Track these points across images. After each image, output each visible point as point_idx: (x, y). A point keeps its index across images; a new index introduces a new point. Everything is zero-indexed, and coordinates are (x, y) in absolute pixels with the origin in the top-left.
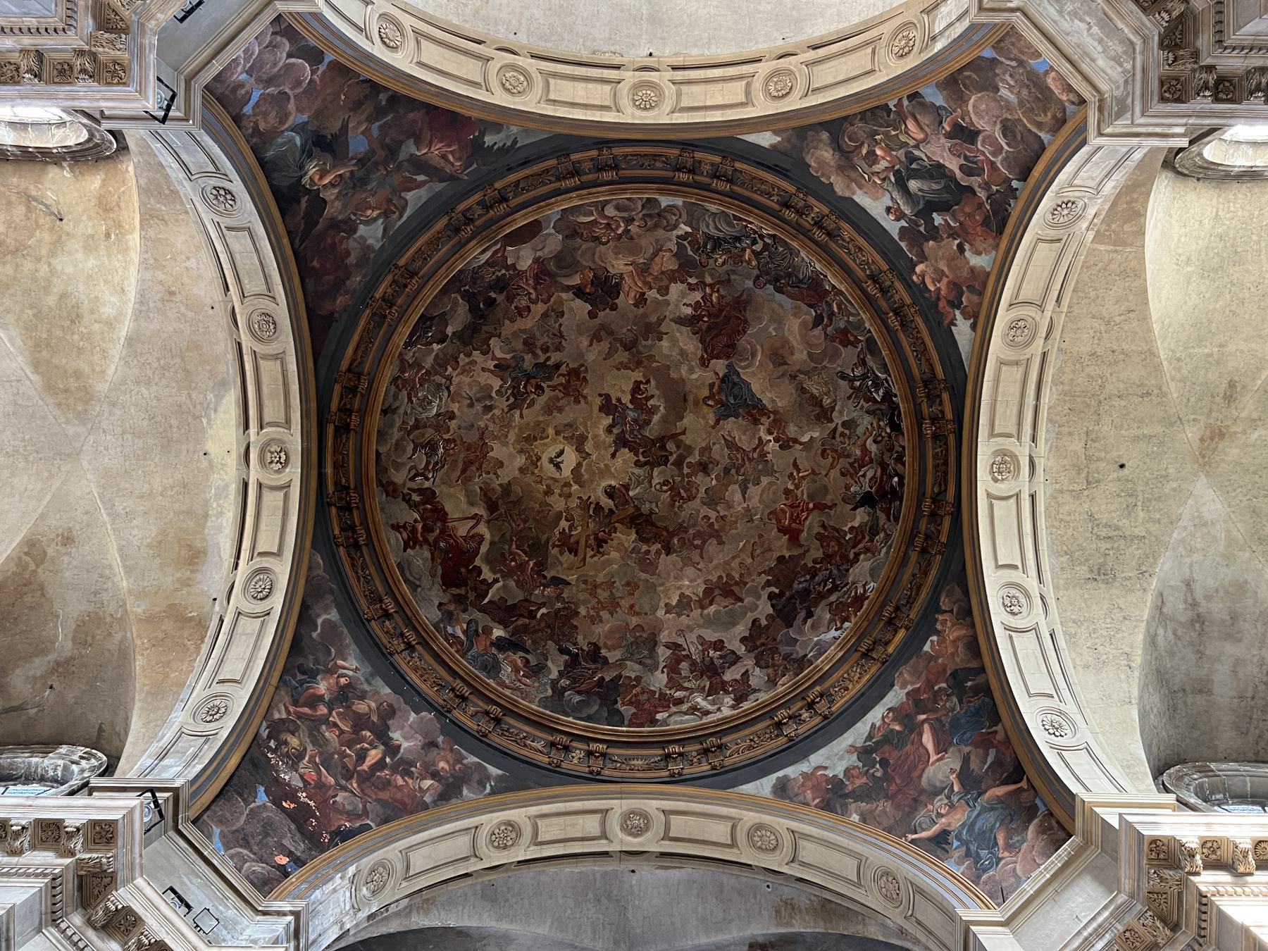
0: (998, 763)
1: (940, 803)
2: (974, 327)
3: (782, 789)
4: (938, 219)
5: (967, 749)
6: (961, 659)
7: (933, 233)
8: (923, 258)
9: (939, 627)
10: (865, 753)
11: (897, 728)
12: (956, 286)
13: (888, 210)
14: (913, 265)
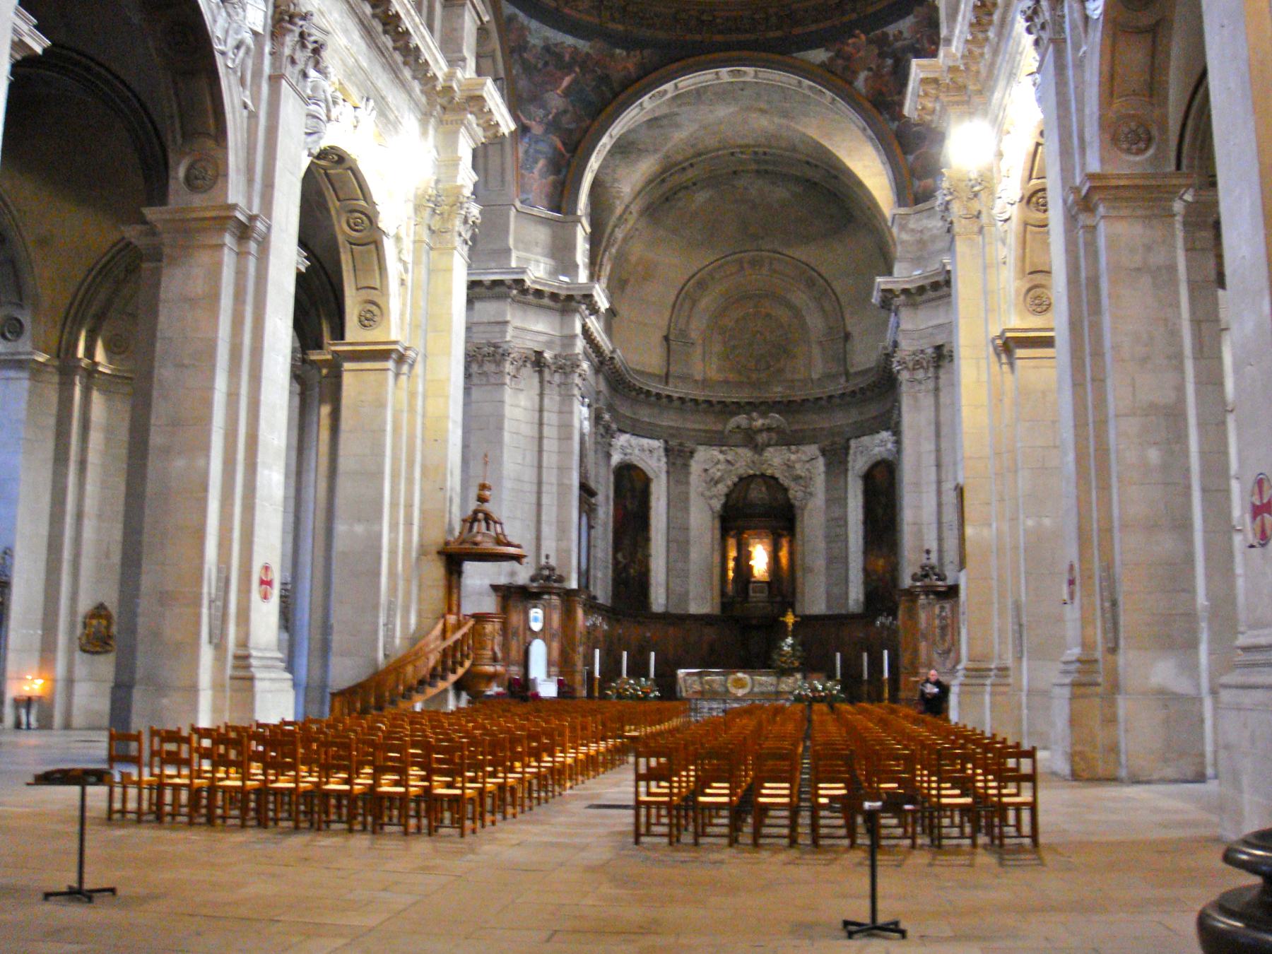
0: (570, 131)
1: (541, 112)
2: (822, 65)
3: (511, 19)
4: (889, 62)
5: (570, 108)
6: (617, 75)
7: (882, 55)
8: (870, 42)
9: (632, 53)
10: (547, 49)
11: (567, 58)
12: (848, 58)
13: (901, 32)
14: (867, 33)
